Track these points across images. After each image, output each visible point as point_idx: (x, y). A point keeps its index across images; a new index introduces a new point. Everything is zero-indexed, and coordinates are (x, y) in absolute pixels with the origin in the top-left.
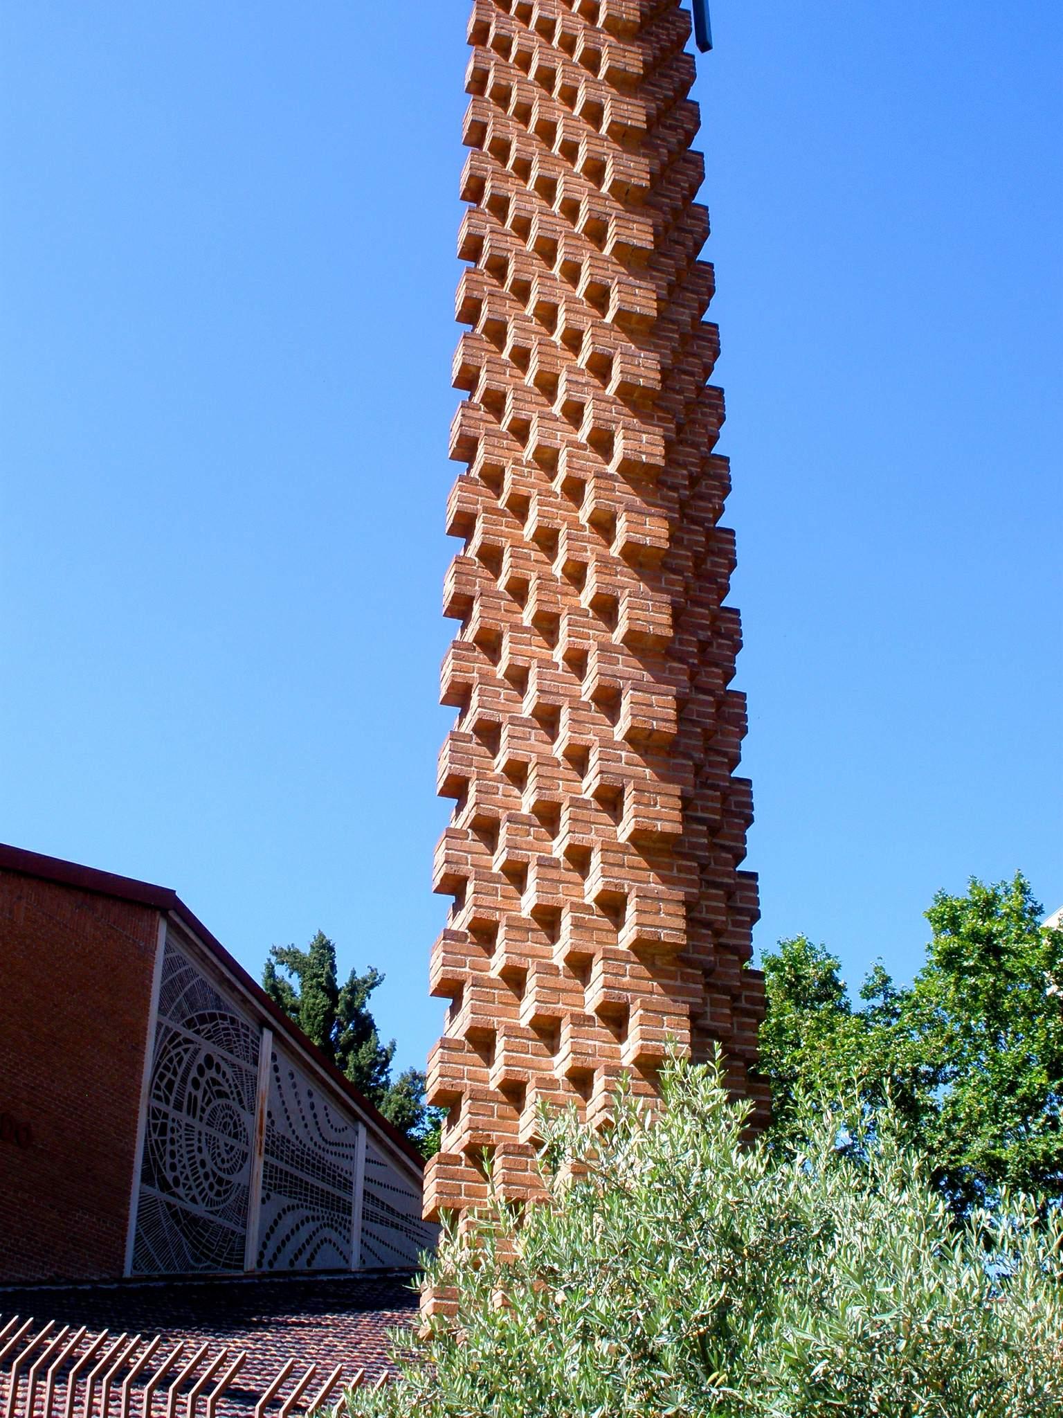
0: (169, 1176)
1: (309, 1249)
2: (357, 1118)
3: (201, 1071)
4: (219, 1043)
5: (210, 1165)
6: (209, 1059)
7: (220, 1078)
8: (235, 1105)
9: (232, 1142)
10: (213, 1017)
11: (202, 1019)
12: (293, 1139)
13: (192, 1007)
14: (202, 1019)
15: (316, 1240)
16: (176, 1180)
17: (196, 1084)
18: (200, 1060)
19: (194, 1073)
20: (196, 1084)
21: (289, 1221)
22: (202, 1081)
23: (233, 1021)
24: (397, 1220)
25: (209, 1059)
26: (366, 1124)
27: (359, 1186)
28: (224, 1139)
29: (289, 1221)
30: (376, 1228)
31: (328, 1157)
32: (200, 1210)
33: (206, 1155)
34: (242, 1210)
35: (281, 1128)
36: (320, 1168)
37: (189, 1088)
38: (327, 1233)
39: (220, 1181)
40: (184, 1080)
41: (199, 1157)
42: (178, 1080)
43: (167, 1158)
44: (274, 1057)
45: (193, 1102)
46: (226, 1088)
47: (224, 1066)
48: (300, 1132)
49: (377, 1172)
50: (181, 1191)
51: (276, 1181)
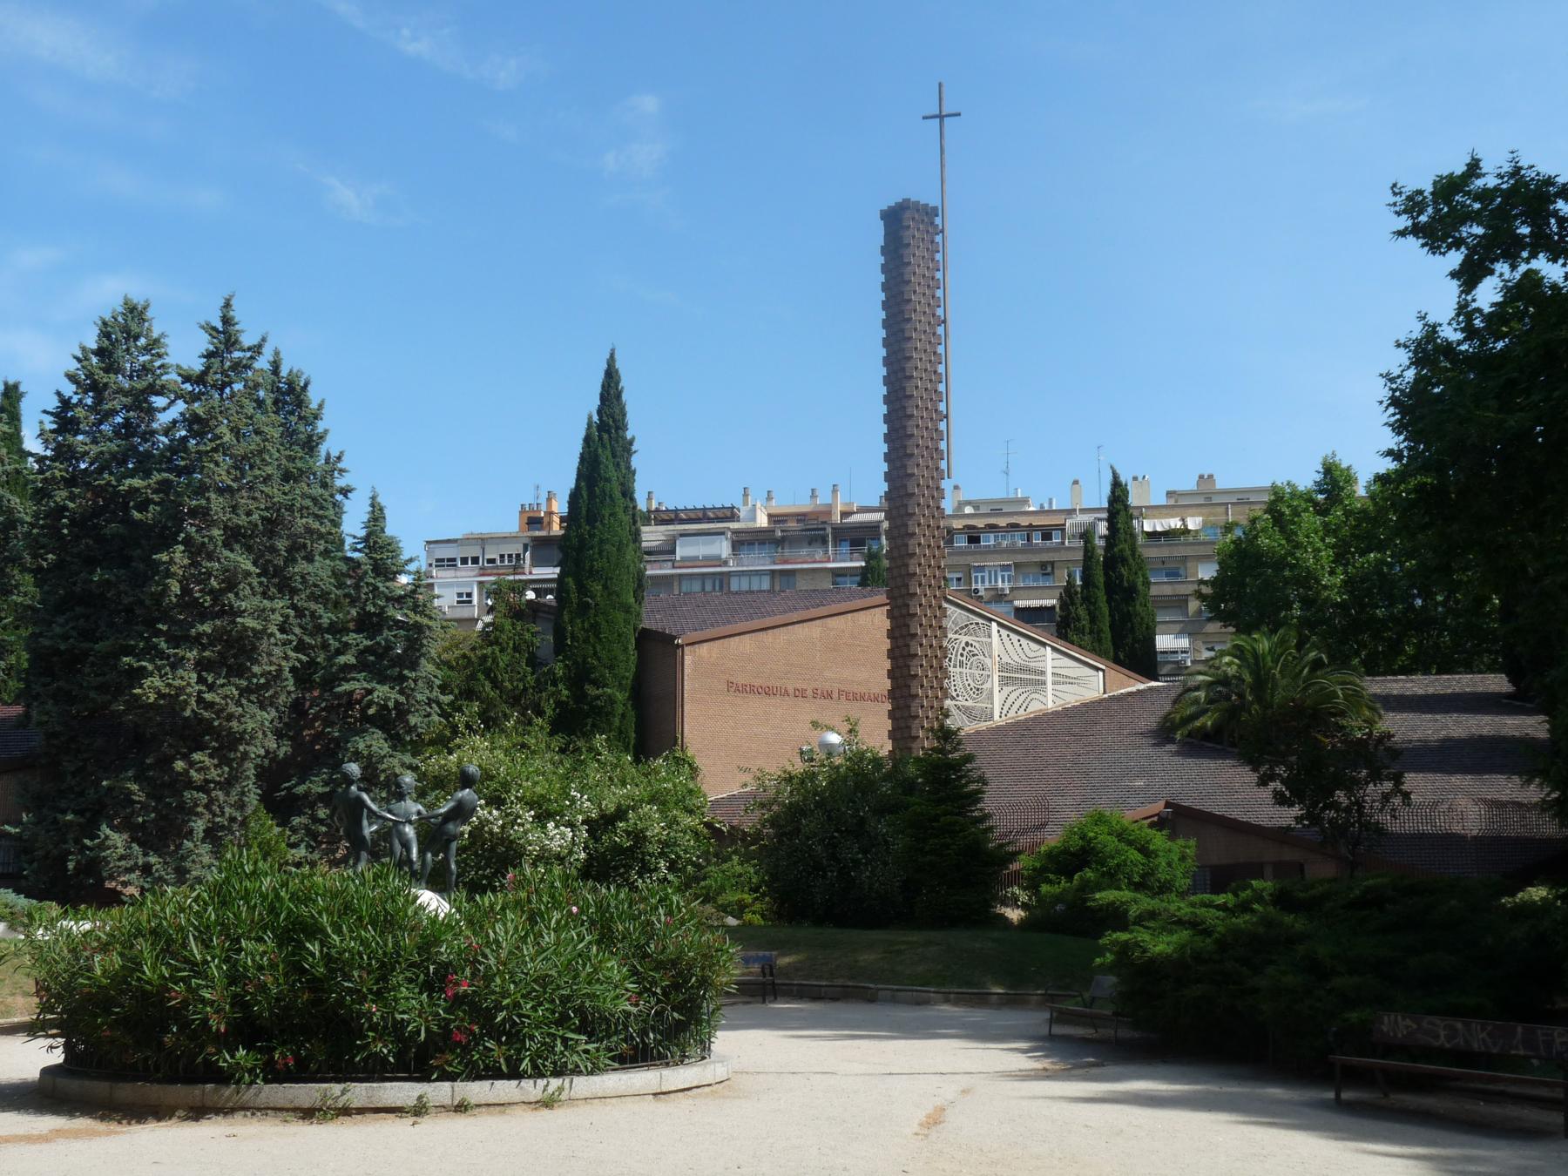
0: (954, 694)
1: (1025, 705)
2: (1044, 645)
3: (964, 649)
4: (971, 635)
5: (972, 685)
6: (967, 644)
7: (973, 649)
8: (982, 657)
9: (982, 672)
10: (966, 626)
11: (962, 628)
12: (1012, 662)
13: (956, 625)
14: (962, 628)
15: (1029, 700)
16: (958, 695)
17: (962, 655)
18: (963, 645)
19: (961, 651)
20: (962, 655)
21: (1013, 696)
22: (965, 653)
23: (977, 624)
24: (1073, 681)
25: (967, 644)
26: (1049, 645)
27: (1049, 671)
28: (977, 672)
29: (1013, 696)
30: (1056, 687)
31: (1031, 664)
32: (970, 703)
33: (970, 681)
34: (990, 697)
35: (1006, 659)
36: (1029, 670)
37: (959, 657)
38: (1034, 696)
39: (978, 690)
40: (956, 656)
41: (967, 683)
42: (953, 657)
43: (953, 688)
44: (999, 631)
45: (961, 663)
46: (976, 652)
47: (974, 644)
48: (1016, 658)
49: (1057, 663)
50: (960, 698)
51: (1004, 681)
